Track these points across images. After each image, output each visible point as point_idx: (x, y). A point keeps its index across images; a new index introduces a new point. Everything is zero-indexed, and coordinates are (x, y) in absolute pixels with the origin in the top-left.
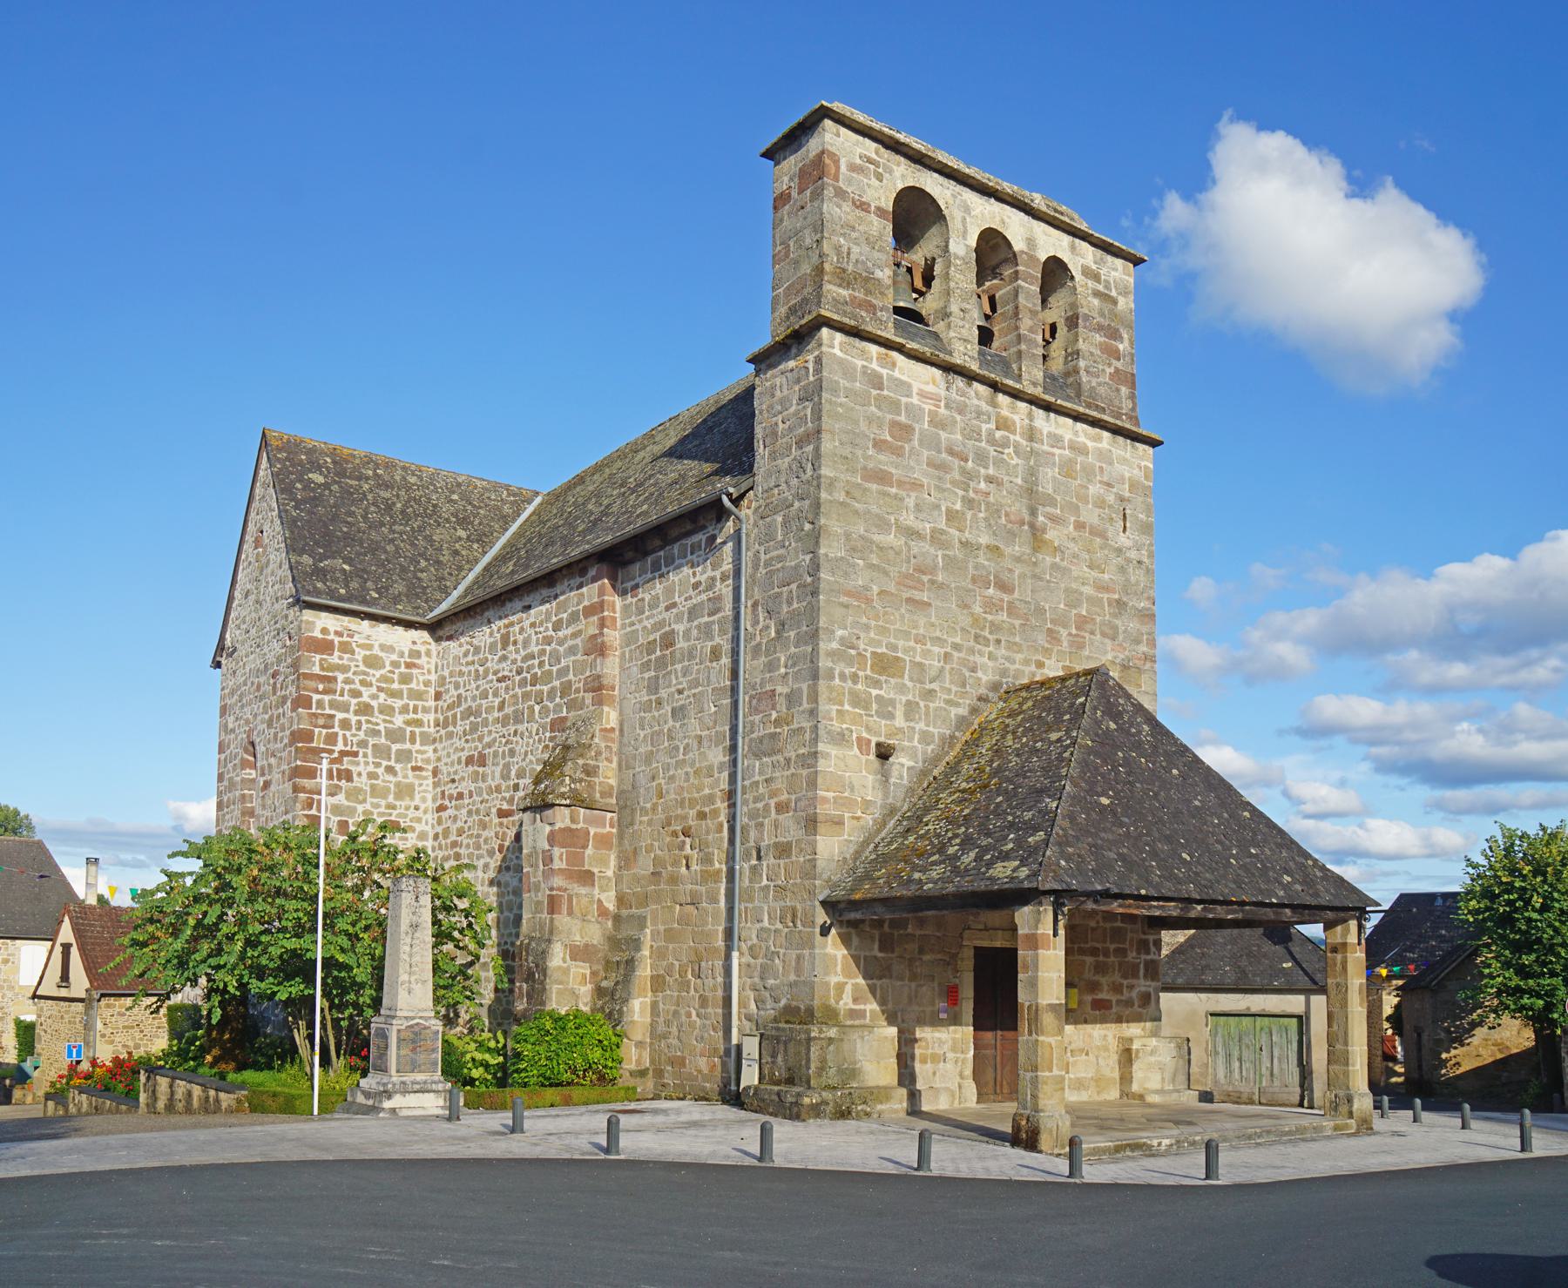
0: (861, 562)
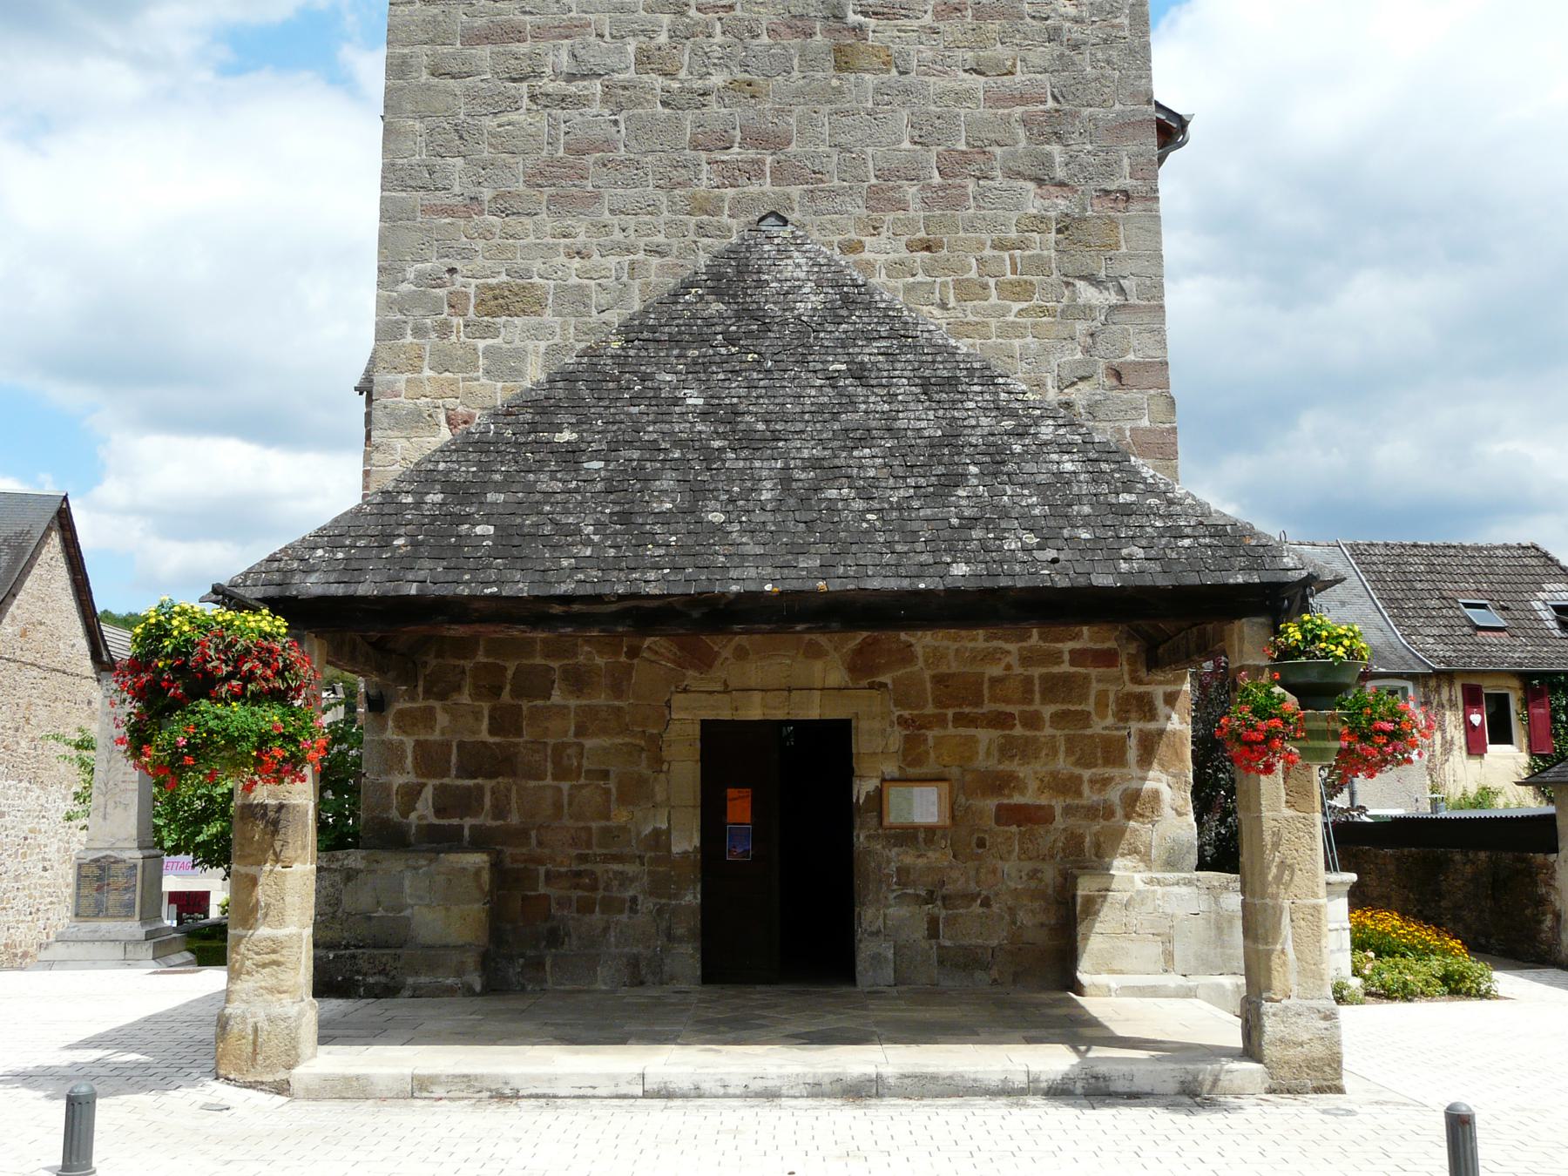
0: (459, 161)
